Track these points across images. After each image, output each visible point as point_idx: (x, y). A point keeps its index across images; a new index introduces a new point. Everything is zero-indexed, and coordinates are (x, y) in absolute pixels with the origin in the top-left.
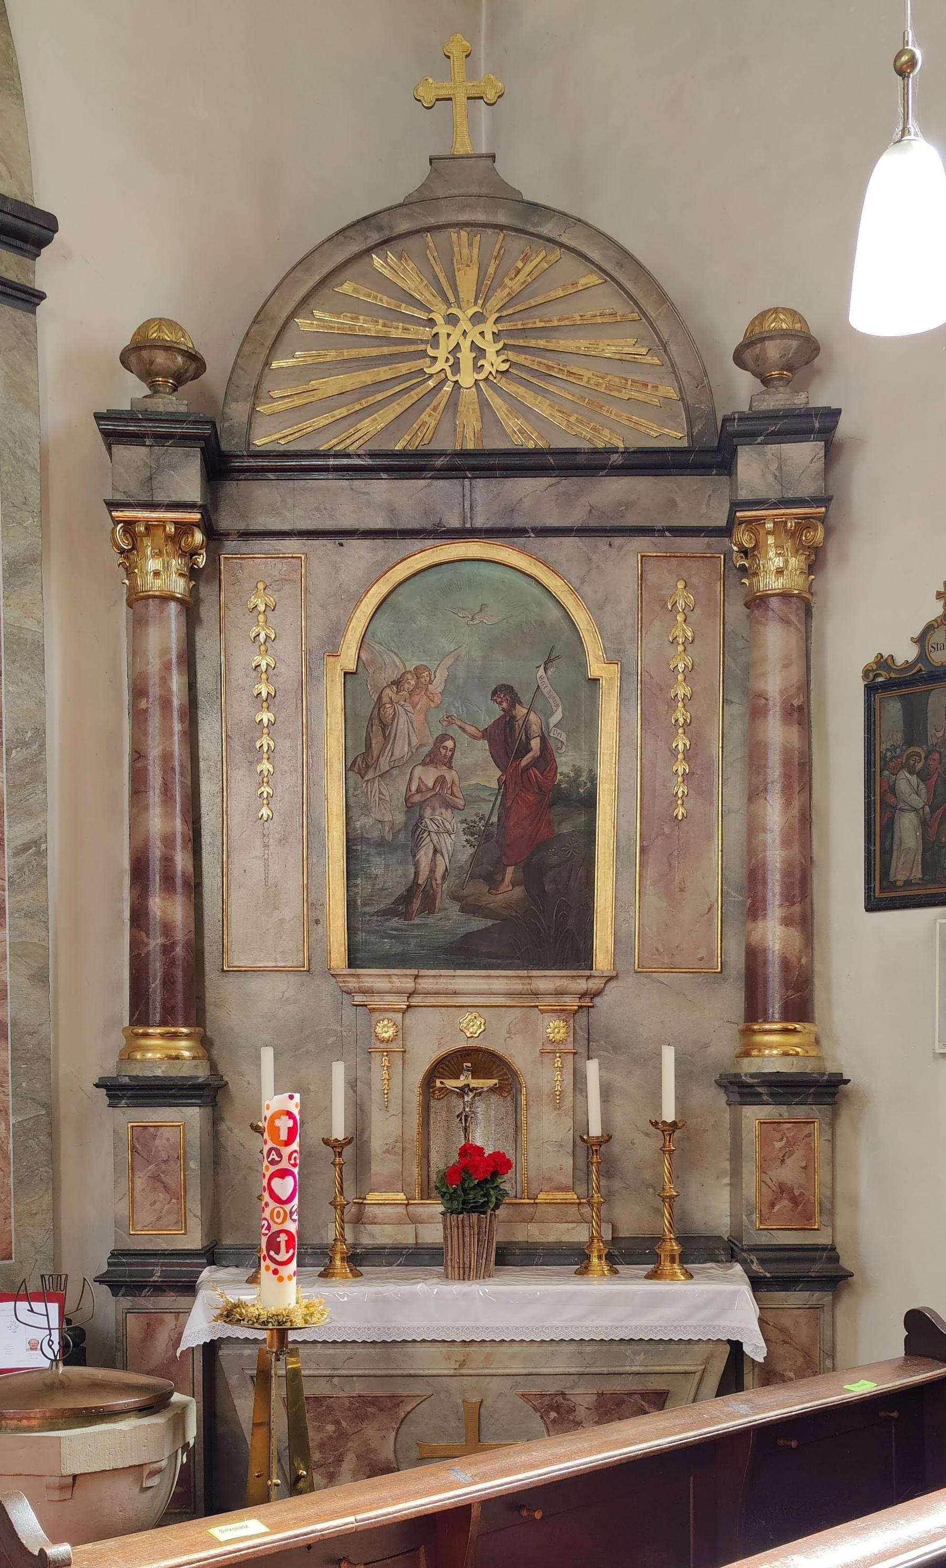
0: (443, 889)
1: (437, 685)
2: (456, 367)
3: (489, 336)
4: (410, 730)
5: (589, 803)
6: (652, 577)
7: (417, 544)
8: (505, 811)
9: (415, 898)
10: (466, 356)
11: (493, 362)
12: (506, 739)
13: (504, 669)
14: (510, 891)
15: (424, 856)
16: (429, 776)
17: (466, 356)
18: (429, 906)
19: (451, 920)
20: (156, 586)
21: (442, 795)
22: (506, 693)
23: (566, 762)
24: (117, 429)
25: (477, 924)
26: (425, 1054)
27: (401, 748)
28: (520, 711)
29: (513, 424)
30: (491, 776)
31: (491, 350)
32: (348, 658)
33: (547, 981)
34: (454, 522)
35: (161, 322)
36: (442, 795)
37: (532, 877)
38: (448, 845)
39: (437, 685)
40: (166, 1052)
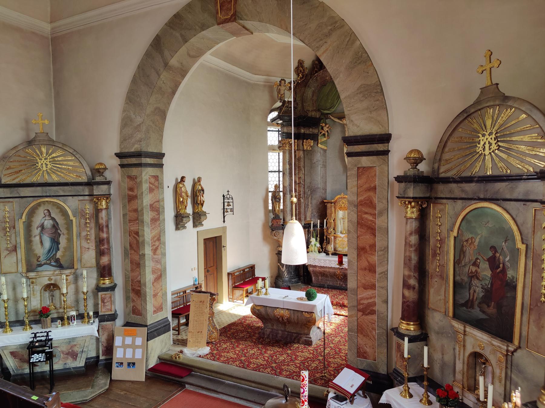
0: (476, 303)
1: (476, 243)
2: (484, 149)
3: (493, 139)
4: (470, 254)
5: (515, 288)
6: (538, 217)
7: (473, 202)
8: (492, 285)
9: (469, 304)
10: (487, 146)
11: (494, 147)
12: (493, 262)
13: (494, 241)
14: (492, 310)
15: (472, 291)
16: (474, 269)
17: (487, 146)
18: (472, 307)
19: (476, 313)
20: (409, 215)
21: (474, 276)
22: (493, 248)
23: (510, 273)
24: (399, 179)
25: (483, 316)
26: (469, 350)
27: (467, 260)
28: (498, 255)
29: (500, 164)
30: (488, 273)
31: (493, 142)
32: (455, 233)
33: (496, 342)
34: (482, 196)
35: (412, 151)
36: (474, 276)
37: (499, 307)
38: (478, 290)
39: (476, 243)
40: (410, 328)
